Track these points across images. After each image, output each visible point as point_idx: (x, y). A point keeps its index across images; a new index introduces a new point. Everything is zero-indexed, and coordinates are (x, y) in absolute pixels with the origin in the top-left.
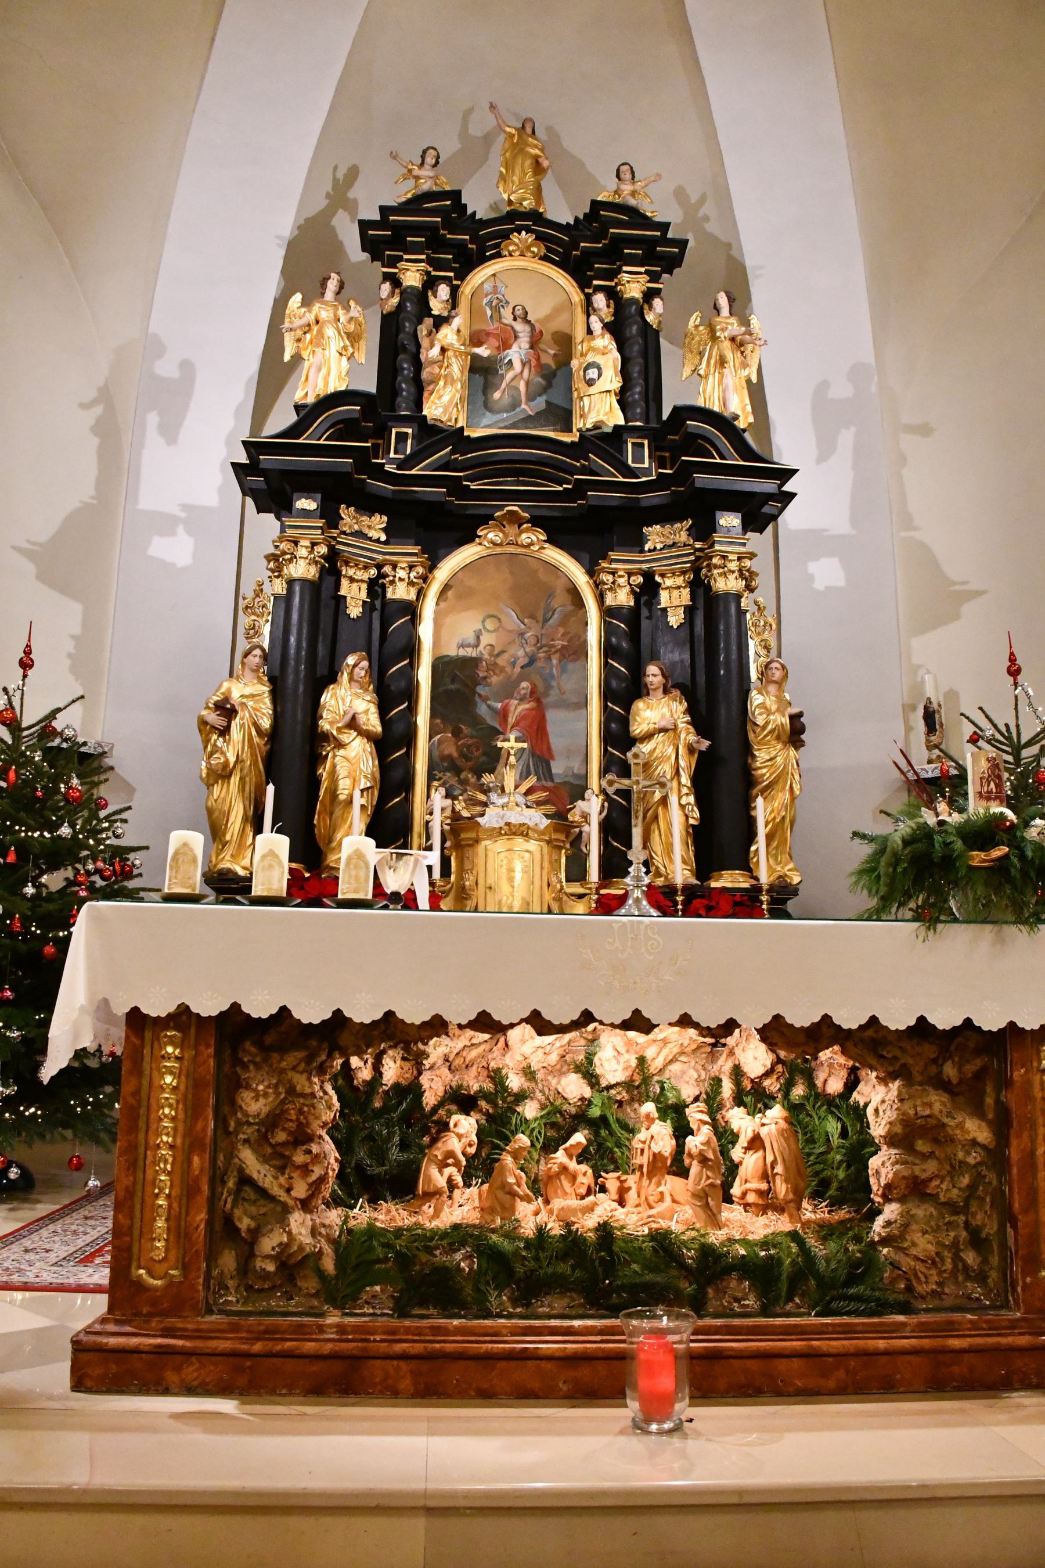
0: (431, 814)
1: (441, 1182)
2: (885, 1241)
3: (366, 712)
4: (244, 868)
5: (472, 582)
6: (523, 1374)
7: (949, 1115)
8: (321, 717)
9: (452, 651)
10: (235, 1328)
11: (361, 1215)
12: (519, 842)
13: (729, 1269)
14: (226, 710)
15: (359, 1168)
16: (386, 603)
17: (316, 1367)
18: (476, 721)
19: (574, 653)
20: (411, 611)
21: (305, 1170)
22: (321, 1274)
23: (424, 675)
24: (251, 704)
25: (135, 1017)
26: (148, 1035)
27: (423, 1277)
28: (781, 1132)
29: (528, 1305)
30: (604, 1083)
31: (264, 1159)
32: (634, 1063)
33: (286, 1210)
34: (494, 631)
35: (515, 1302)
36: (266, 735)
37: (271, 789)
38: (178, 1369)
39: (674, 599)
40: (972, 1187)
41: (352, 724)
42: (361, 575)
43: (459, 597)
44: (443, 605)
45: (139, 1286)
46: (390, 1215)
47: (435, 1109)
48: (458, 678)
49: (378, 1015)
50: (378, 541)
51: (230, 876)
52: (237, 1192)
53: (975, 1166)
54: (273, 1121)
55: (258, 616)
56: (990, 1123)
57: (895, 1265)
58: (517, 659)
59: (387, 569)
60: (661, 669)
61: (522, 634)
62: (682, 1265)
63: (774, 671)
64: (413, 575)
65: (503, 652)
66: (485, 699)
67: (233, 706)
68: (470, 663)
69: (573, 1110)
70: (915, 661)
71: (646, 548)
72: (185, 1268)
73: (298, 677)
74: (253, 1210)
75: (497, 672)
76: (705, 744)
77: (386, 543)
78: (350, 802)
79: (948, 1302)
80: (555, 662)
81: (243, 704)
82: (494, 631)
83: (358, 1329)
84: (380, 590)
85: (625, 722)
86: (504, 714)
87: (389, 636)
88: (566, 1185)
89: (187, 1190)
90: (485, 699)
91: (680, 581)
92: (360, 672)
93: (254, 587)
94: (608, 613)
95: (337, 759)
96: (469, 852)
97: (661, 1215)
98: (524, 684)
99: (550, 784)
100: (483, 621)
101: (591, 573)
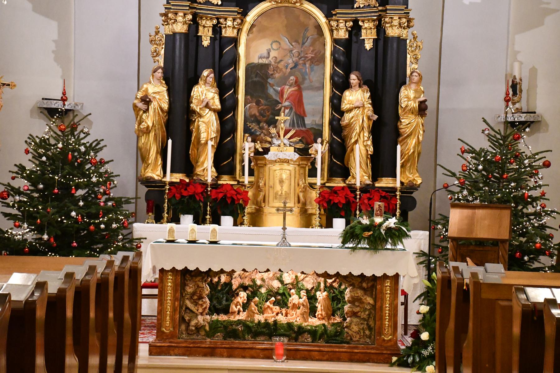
0: (244, 150)
1: (236, 310)
2: (347, 327)
3: (213, 98)
4: (158, 176)
5: (265, 22)
6: (253, 352)
7: (363, 296)
8: (192, 102)
9: (255, 60)
10: (186, 342)
11: (215, 317)
12: (285, 166)
13: (305, 332)
14: (146, 101)
15: (214, 306)
16: (221, 38)
17: (205, 350)
18: (268, 97)
19: (317, 61)
20: (235, 41)
21: (202, 305)
22: (205, 330)
23: (241, 73)
24: (158, 97)
25: (162, 271)
26: (164, 273)
27: (230, 332)
28: (324, 299)
29: (255, 338)
30: (285, 283)
31: (192, 303)
32: (294, 277)
33: (197, 315)
34: (277, 49)
35: (252, 338)
36: (166, 112)
37: (170, 141)
38: (173, 350)
39: (368, 37)
40: (369, 315)
41: (207, 106)
42: (209, 23)
43: (259, 31)
44: (251, 35)
45: (163, 332)
46: (223, 317)
47: (236, 290)
48: (259, 75)
49: (219, 270)
50: (217, 5)
51: (152, 180)
52: (185, 311)
53: (369, 309)
54: (194, 294)
55: (157, 45)
56: (373, 299)
57: (347, 333)
58: (288, 64)
59: (221, 20)
60: (357, 76)
61: (291, 51)
62: (293, 330)
63: (414, 77)
64: (235, 23)
65: (281, 61)
66: (272, 86)
67: (150, 99)
68: (267, 66)
69: (276, 291)
70: (517, 48)
71: (355, 7)
72: (174, 328)
73: (180, 80)
74: (189, 315)
75: (278, 71)
76: (376, 117)
77: (221, 5)
78: (206, 143)
79: (361, 342)
80: (307, 65)
81: (154, 98)
82: (277, 49)
83: (214, 342)
84: (218, 29)
85: (340, 99)
86: (282, 93)
87: (223, 55)
88: (270, 311)
89: (174, 310)
90: (272, 86)
91: (371, 25)
92: (211, 79)
93: (155, 30)
94: (336, 41)
95: (200, 122)
96: (261, 170)
97: (291, 319)
98: (292, 78)
99: (304, 129)
100: (271, 44)
101: (328, 16)
